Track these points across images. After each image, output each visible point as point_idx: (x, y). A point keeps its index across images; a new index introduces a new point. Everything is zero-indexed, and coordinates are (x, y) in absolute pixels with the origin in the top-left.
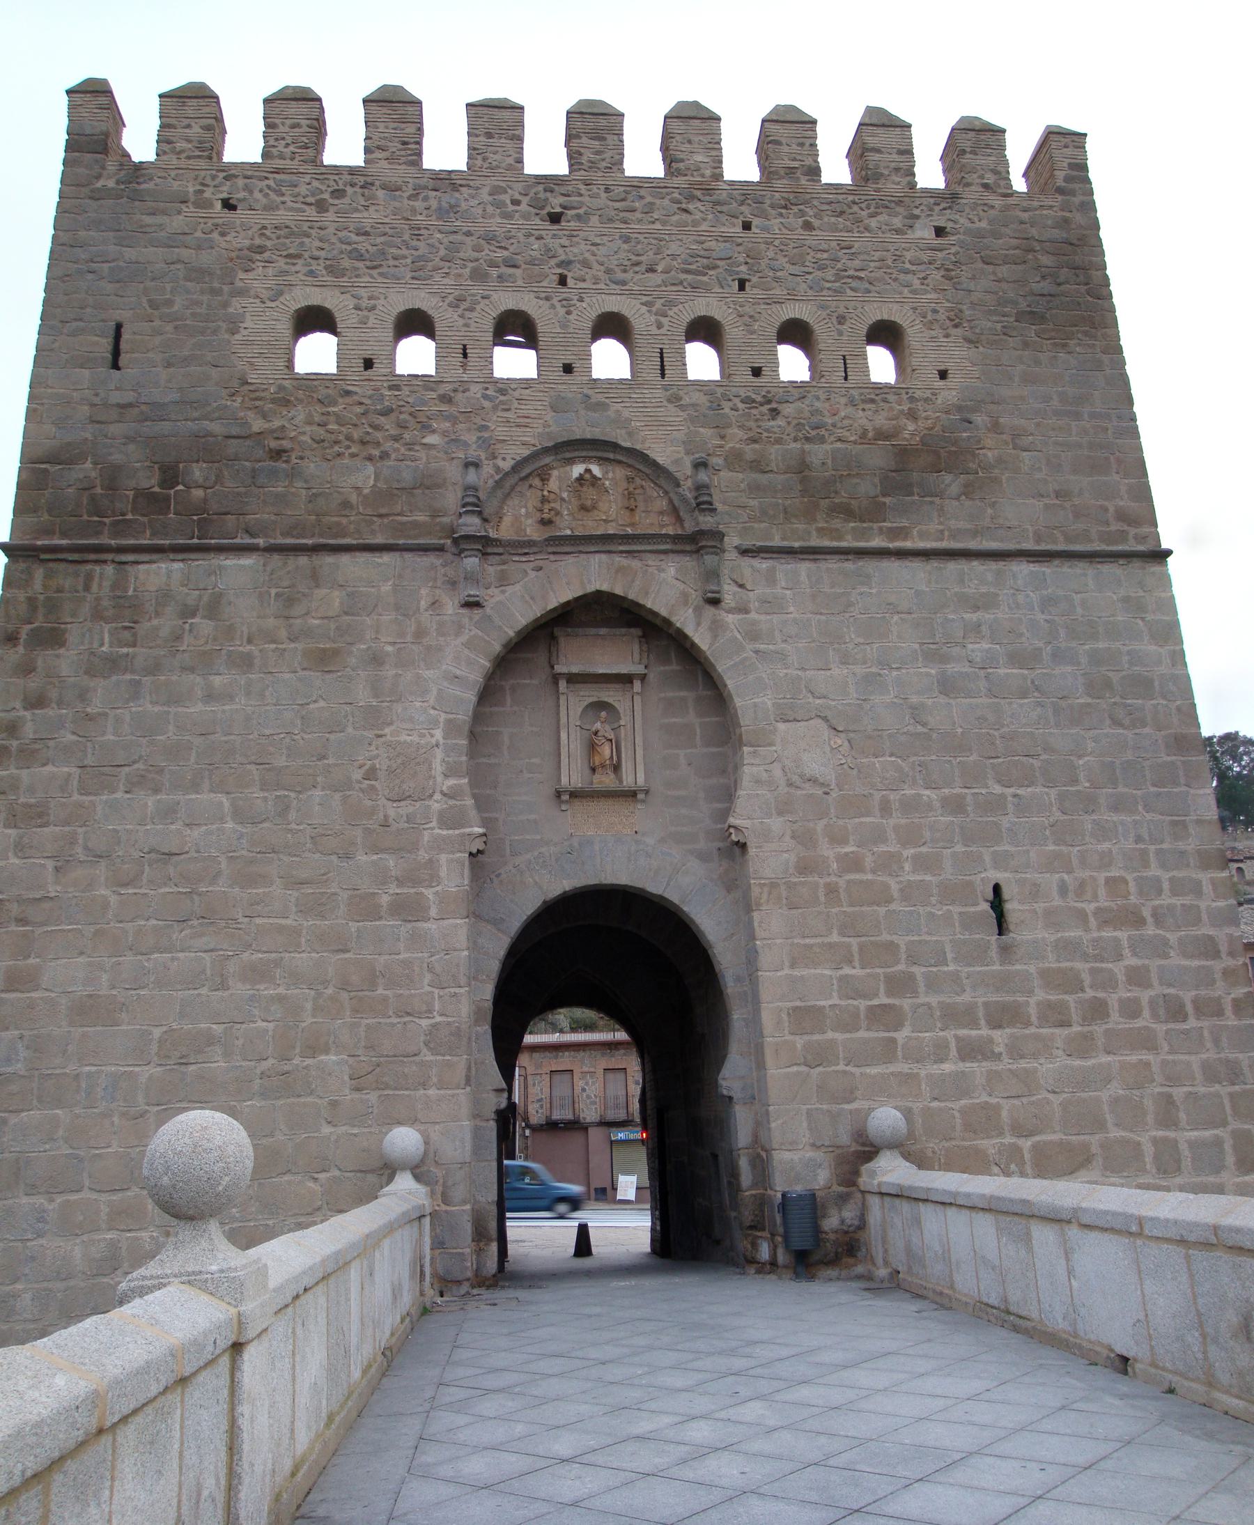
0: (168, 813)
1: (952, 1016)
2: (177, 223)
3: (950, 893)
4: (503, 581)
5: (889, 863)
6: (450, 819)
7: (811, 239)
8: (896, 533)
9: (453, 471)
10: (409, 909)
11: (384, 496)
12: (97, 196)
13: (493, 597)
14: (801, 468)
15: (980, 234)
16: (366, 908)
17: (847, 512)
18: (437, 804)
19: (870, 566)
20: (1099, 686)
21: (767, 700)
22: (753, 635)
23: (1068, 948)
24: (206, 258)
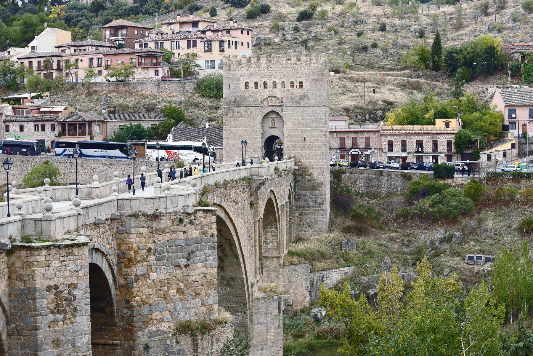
0: (238, 130)
1: (300, 147)
2: (234, 73)
3: (301, 137)
4: (264, 109)
5: (296, 135)
6: (260, 131)
7: (295, 71)
8: (299, 104)
9: (260, 99)
10: (257, 138)
11: (254, 101)
12: (226, 70)
13: (263, 111)
14: (291, 97)
15: (312, 70)
16: (253, 138)
17: (295, 102)
18: (259, 129)
19: (297, 107)
20: (317, 119)
21: (287, 120)
22: (286, 114)
23: (311, 142)
24: (237, 77)
